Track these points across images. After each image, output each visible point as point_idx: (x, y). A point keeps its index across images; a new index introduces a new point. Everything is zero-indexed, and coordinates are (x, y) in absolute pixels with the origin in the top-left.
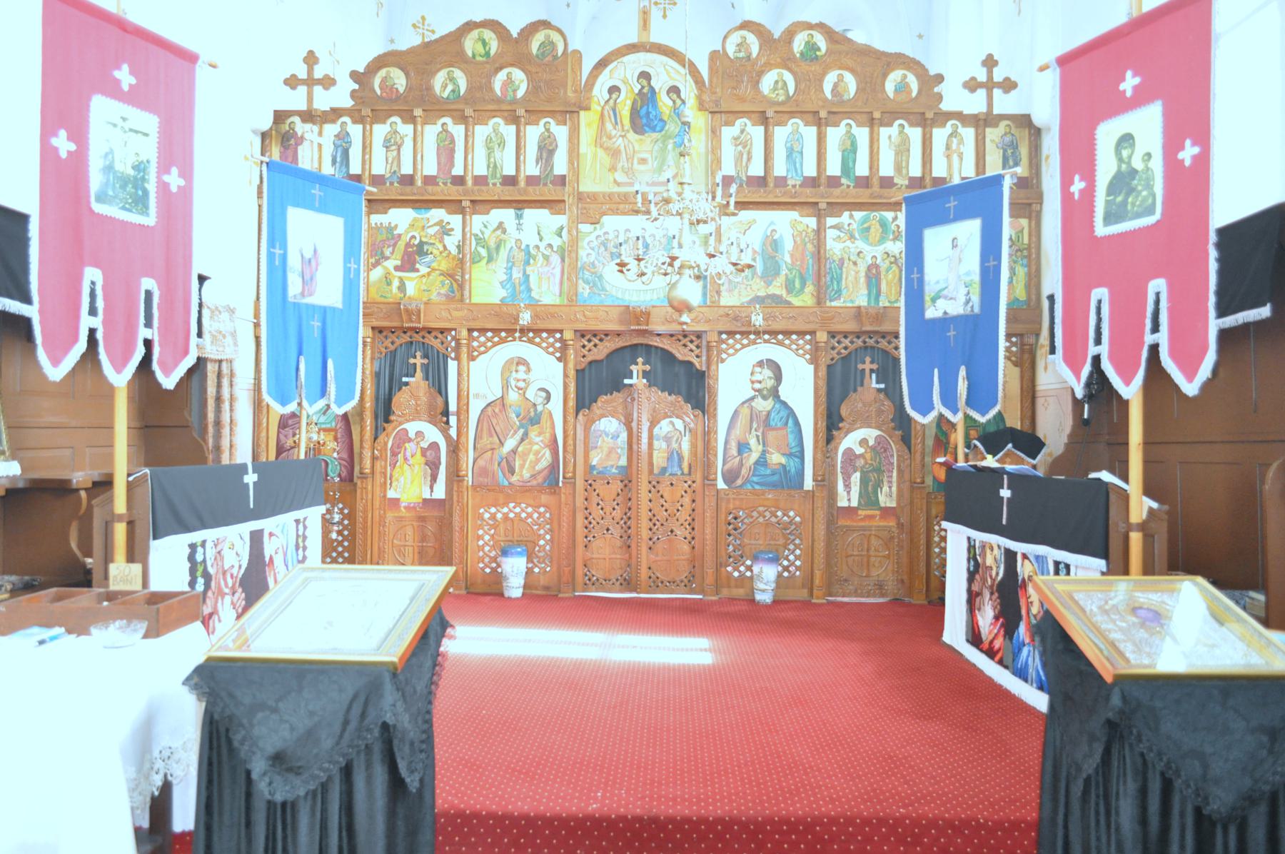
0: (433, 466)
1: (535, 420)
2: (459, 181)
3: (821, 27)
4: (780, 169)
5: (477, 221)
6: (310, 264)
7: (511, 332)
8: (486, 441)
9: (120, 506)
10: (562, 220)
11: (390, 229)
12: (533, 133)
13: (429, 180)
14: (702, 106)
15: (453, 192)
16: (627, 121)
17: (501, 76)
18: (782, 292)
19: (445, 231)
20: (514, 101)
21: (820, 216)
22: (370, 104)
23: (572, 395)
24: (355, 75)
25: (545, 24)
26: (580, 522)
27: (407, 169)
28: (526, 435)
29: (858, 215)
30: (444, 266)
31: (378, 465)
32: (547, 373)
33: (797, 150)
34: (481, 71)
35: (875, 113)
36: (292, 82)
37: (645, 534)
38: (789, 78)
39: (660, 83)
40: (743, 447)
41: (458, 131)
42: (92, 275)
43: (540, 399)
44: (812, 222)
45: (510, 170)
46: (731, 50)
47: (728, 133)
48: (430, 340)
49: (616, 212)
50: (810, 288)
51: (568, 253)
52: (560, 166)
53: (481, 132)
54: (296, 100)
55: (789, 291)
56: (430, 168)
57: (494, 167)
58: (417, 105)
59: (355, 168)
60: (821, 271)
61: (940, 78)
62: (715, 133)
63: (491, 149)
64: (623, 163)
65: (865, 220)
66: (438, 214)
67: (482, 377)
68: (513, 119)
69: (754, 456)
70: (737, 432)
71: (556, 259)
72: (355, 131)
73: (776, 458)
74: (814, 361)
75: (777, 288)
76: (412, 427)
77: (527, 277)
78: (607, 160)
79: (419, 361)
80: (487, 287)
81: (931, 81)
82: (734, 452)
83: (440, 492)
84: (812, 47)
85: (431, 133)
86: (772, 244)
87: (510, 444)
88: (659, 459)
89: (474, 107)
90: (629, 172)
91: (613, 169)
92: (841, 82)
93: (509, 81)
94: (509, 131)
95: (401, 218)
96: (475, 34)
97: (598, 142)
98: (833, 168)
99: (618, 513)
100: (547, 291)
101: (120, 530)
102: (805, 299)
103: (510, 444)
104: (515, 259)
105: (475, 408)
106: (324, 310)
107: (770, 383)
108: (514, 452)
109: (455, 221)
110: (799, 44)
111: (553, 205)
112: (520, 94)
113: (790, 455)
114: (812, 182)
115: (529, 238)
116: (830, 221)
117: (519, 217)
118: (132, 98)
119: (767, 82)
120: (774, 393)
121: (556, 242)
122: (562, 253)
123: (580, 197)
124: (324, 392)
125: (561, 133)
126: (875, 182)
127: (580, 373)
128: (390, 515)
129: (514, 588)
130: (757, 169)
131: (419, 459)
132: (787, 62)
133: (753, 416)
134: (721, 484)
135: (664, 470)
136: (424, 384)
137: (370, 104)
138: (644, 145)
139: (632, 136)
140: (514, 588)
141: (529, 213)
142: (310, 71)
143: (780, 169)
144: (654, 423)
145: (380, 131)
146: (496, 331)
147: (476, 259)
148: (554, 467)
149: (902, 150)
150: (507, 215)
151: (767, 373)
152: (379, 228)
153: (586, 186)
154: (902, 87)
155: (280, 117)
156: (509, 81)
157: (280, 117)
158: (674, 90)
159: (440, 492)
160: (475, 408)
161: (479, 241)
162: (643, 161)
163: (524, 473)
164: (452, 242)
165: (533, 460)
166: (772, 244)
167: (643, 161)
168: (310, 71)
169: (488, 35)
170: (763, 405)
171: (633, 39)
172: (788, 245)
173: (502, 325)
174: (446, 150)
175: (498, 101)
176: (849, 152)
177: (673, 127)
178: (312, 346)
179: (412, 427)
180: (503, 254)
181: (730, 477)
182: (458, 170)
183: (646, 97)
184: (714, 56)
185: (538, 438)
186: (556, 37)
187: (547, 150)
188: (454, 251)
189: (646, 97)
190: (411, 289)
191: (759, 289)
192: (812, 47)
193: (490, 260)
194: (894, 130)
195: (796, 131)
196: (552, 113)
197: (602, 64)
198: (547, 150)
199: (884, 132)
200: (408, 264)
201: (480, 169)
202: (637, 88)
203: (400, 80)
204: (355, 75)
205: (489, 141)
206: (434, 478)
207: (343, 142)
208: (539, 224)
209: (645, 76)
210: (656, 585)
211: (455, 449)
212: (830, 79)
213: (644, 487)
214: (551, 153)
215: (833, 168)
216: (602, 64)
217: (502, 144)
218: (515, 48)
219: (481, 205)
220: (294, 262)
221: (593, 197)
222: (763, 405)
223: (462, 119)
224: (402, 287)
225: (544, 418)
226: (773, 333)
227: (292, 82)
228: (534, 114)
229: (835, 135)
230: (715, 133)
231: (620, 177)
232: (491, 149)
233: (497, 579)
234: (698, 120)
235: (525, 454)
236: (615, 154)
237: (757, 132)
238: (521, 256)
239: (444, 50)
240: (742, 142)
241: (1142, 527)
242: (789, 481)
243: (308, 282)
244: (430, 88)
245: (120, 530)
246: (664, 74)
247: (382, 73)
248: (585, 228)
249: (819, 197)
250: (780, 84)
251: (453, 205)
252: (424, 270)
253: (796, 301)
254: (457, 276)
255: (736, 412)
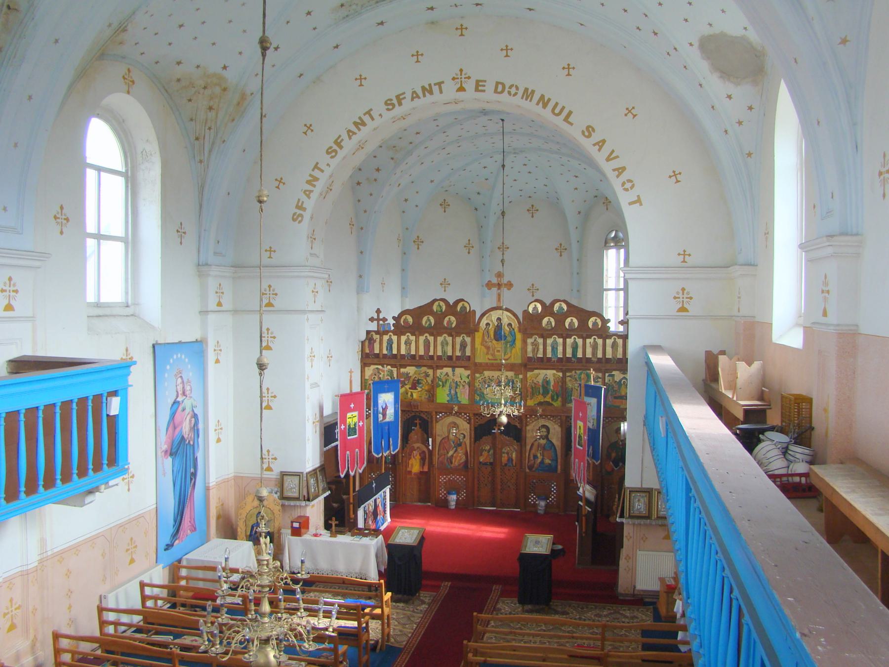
0: (423, 460)
1: (460, 445)
2: (432, 357)
3: (565, 301)
4: (549, 355)
5: (439, 371)
6: (385, 410)
7: (451, 413)
8: (442, 451)
9: (351, 501)
10: (468, 372)
11: (407, 374)
12: (459, 340)
13: (421, 357)
14: (520, 331)
15: (430, 363)
16: (492, 336)
17: (447, 319)
18: (550, 400)
19: (427, 375)
20: (452, 329)
21: (564, 373)
22: (400, 329)
23: (473, 436)
24: (394, 318)
25: (462, 300)
26: (476, 480)
27: (413, 352)
28: (456, 451)
29: (578, 372)
30: (427, 388)
31: (404, 459)
32: (465, 426)
33: (557, 347)
34: (440, 317)
35: (584, 332)
36: (372, 320)
37: (499, 487)
38: (552, 320)
39: (505, 321)
40: (535, 457)
41: (431, 339)
42: (348, 452)
43: (461, 437)
44: (561, 374)
45: (450, 353)
46: (530, 310)
47: (530, 341)
48: (422, 415)
49: (489, 370)
50: (560, 399)
51: (471, 385)
52: (468, 353)
53: (440, 339)
54: (373, 326)
55: (552, 399)
56: (422, 352)
57: (444, 352)
58: (417, 329)
59: (395, 352)
60: (564, 393)
61: (609, 321)
62: (525, 342)
63: (444, 345)
64: (491, 351)
65: (581, 374)
66: (424, 369)
67: (441, 428)
68: (450, 335)
69: (539, 460)
70: (533, 451)
71: (467, 387)
72: (395, 338)
73: (547, 461)
74: (561, 426)
75: (548, 399)
76: (416, 445)
77: (456, 393)
78: (485, 350)
79: (417, 421)
80: (442, 396)
81: (605, 322)
82: (532, 458)
83: (426, 469)
84: (561, 308)
85: (422, 339)
86: (546, 382)
87: (451, 453)
88: (505, 458)
89: (437, 330)
90: (493, 355)
91: (487, 354)
92: (572, 321)
93: (449, 322)
94: (449, 339)
95: (411, 370)
96: (436, 303)
97: (482, 344)
98: (569, 354)
99: (490, 479)
100: (464, 399)
101: (351, 506)
102: (557, 404)
103: (451, 453)
104: (452, 387)
105: (439, 439)
106: (389, 423)
107: (545, 434)
108: (452, 456)
109: (430, 372)
110: (556, 307)
111: (466, 368)
112: (453, 326)
113: (552, 460)
114: (560, 360)
115: (458, 379)
116: (568, 374)
117: (453, 371)
118: (354, 410)
119: (545, 321)
120: (547, 437)
121: (467, 380)
122: (469, 384)
123: (475, 364)
124: (389, 448)
125: (468, 340)
126: (584, 361)
127: (476, 429)
128: (408, 476)
129: (453, 505)
130: (540, 355)
131: (418, 457)
132: (552, 314)
133: (539, 445)
134: (527, 470)
135: (506, 465)
136: (420, 430)
137: (400, 329)
138: (499, 345)
139: (494, 342)
140: (453, 505)
141: (457, 369)
142: (378, 316)
143: (549, 355)
144: (502, 448)
145: (403, 338)
146: (446, 413)
147: (438, 386)
148: (466, 462)
149: (595, 347)
150: (449, 370)
151: (544, 430)
152: (403, 373)
153: (479, 360)
154: (595, 324)
155: (368, 332)
156: (449, 322)
157: (368, 332)
158: (510, 325)
159: (426, 469)
160: (439, 439)
161: (440, 379)
162: (498, 351)
163: (456, 463)
164: (429, 379)
165: (459, 458)
166: (546, 382)
167: (498, 351)
168: (378, 316)
169: (442, 303)
170: (543, 442)
171: (495, 305)
172: (552, 383)
173: (447, 410)
174: (427, 344)
175: (446, 328)
176: (575, 347)
177: (509, 339)
178: (386, 436)
179: (416, 445)
180: (448, 384)
181: (530, 468)
182: (431, 353)
183: (499, 327)
184: (526, 312)
185: (461, 452)
186: (466, 305)
187: (463, 346)
188: (430, 382)
189: (499, 327)
190: (415, 396)
191: (540, 398)
192: (561, 308)
193: (443, 386)
194: (592, 340)
195: (555, 340)
196: (466, 334)
197: (483, 315)
198: (463, 346)
199: (588, 341)
200: (414, 387)
201: (439, 353)
202: (496, 324)
203: (410, 320)
204: (394, 318)
205: (442, 343)
206: (424, 464)
207: (390, 342)
208: (462, 374)
209: (499, 319)
210: (503, 506)
211: (431, 453)
212: (568, 320)
213: (498, 470)
214: (465, 347)
215: (569, 354)
216: (483, 315)
217: (447, 344)
218: (451, 309)
219: (442, 367)
220: (380, 410)
221: (481, 364)
222: (543, 442)
223: (431, 334)
224: (412, 395)
225: (463, 445)
226: (547, 416)
227: (372, 320)
228: (458, 334)
229: (569, 341)
230: (525, 342)
231: (491, 357)
232: (444, 345)
233: (446, 502)
234: (519, 336)
235: (456, 458)
236: (488, 348)
237: (541, 341)
238: (454, 385)
239: (426, 309)
240: (535, 345)
241: (585, 515)
242: (552, 469)
243: (384, 415)
244: (421, 324)
245: (351, 506)
246: (506, 318)
247: (404, 317)
248: (477, 375)
249: (564, 364)
250: (549, 323)
251: (430, 367)
252: (419, 389)
253: (555, 404)
254: (432, 394)
255: (532, 445)
